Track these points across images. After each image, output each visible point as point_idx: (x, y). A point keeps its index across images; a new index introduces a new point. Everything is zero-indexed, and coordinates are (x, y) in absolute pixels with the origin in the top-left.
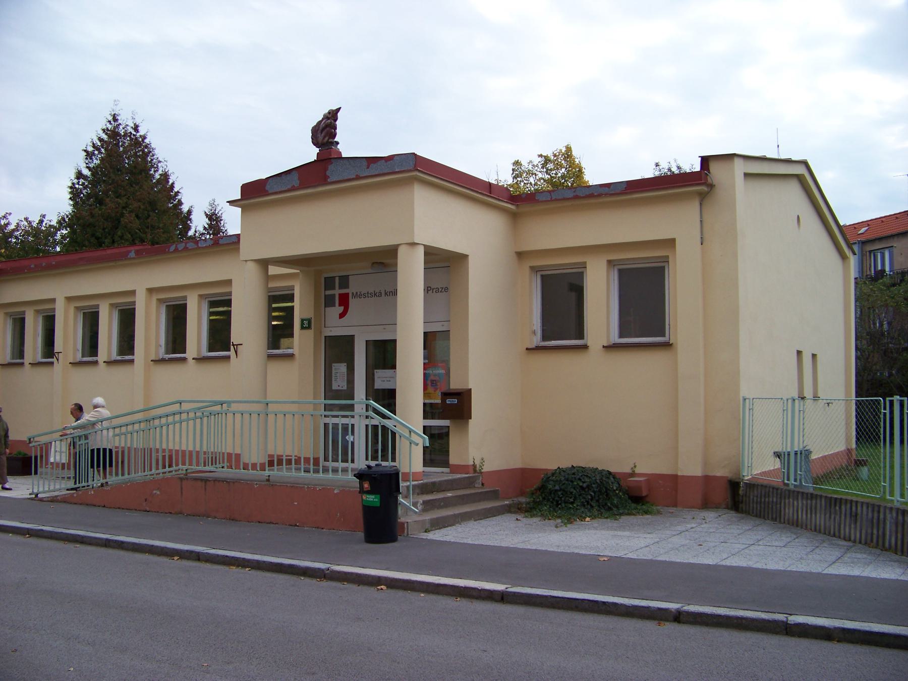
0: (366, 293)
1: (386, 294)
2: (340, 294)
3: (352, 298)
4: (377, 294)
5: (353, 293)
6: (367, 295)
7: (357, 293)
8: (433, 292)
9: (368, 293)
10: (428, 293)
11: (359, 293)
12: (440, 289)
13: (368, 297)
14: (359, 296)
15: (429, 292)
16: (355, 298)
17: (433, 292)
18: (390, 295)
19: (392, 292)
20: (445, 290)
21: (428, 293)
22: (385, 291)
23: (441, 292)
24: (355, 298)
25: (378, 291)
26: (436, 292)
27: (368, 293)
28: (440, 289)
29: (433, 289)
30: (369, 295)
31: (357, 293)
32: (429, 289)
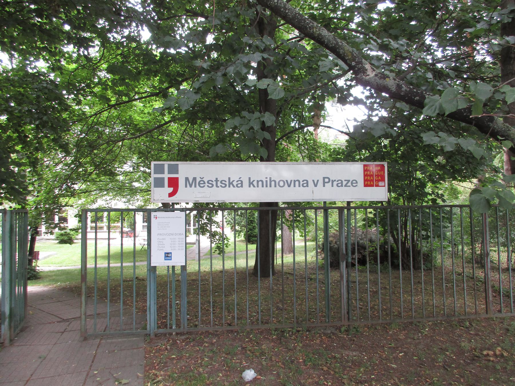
0: (214, 179)
1: (251, 183)
2: (169, 178)
3: (186, 186)
4: (235, 183)
5: (187, 179)
6: (214, 183)
7: (195, 179)
8: (332, 186)
9: (217, 180)
10: (324, 186)
11: (198, 180)
12: (344, 183)
13: (217, 186)
14: (199, 184)
15: (326, 184)
16: (191, 186)
17: (332, 186)
18: (258, 186)
19: (262, 181)
20: (352, 183)
21: (324, 186)
22: (250, 178)
23: (346, 186)
24: (191, 186)
25: (235, 178)
26: (337, 185)
27: (217, 180)
28: (344, 183)
29: (333, 181)
30: (219, 184)
31: (195, 179)
32: (327, 180)
